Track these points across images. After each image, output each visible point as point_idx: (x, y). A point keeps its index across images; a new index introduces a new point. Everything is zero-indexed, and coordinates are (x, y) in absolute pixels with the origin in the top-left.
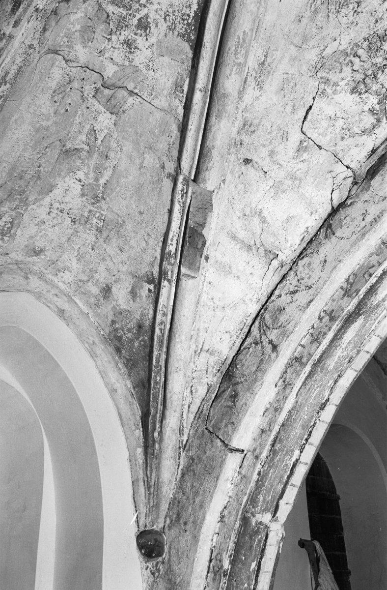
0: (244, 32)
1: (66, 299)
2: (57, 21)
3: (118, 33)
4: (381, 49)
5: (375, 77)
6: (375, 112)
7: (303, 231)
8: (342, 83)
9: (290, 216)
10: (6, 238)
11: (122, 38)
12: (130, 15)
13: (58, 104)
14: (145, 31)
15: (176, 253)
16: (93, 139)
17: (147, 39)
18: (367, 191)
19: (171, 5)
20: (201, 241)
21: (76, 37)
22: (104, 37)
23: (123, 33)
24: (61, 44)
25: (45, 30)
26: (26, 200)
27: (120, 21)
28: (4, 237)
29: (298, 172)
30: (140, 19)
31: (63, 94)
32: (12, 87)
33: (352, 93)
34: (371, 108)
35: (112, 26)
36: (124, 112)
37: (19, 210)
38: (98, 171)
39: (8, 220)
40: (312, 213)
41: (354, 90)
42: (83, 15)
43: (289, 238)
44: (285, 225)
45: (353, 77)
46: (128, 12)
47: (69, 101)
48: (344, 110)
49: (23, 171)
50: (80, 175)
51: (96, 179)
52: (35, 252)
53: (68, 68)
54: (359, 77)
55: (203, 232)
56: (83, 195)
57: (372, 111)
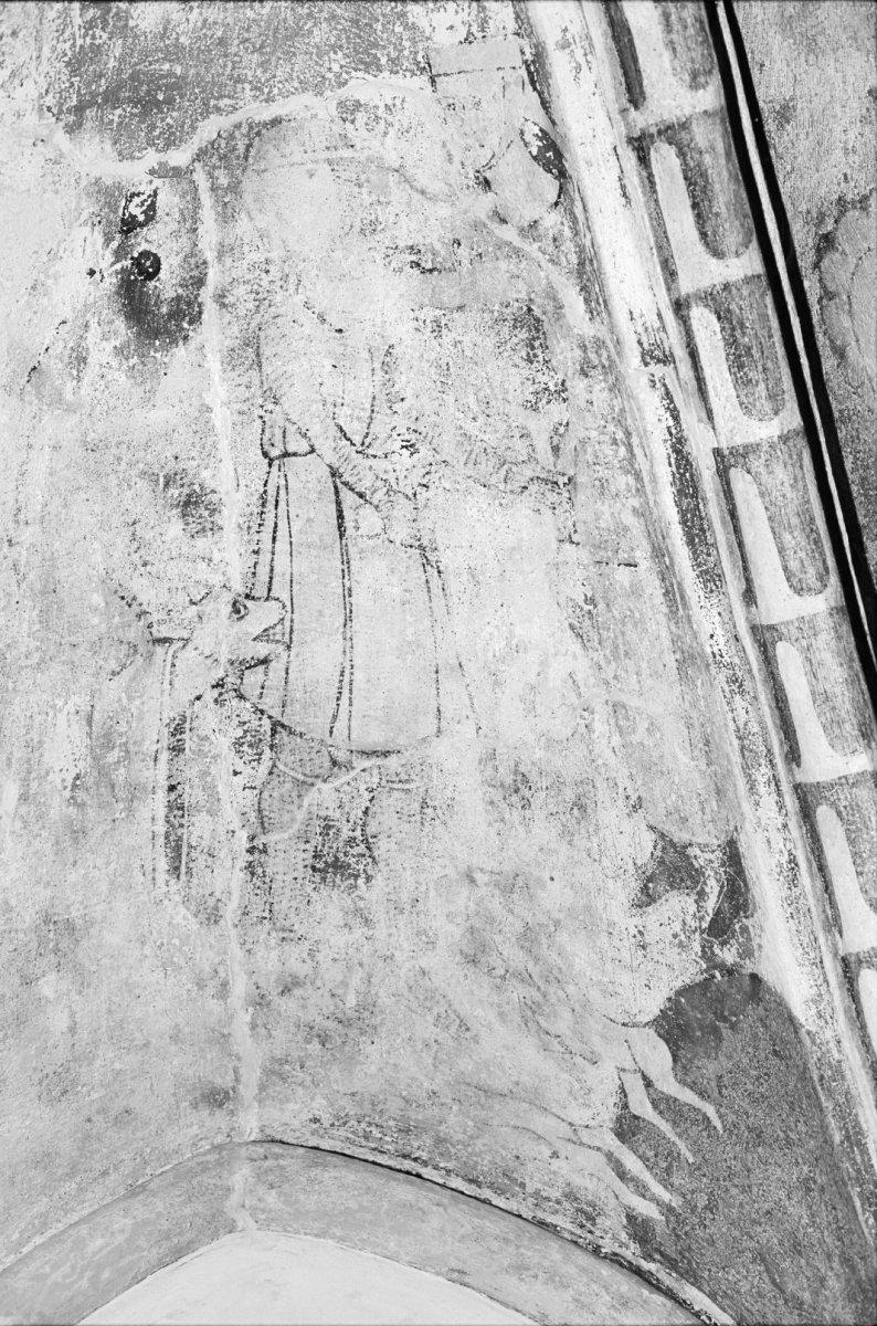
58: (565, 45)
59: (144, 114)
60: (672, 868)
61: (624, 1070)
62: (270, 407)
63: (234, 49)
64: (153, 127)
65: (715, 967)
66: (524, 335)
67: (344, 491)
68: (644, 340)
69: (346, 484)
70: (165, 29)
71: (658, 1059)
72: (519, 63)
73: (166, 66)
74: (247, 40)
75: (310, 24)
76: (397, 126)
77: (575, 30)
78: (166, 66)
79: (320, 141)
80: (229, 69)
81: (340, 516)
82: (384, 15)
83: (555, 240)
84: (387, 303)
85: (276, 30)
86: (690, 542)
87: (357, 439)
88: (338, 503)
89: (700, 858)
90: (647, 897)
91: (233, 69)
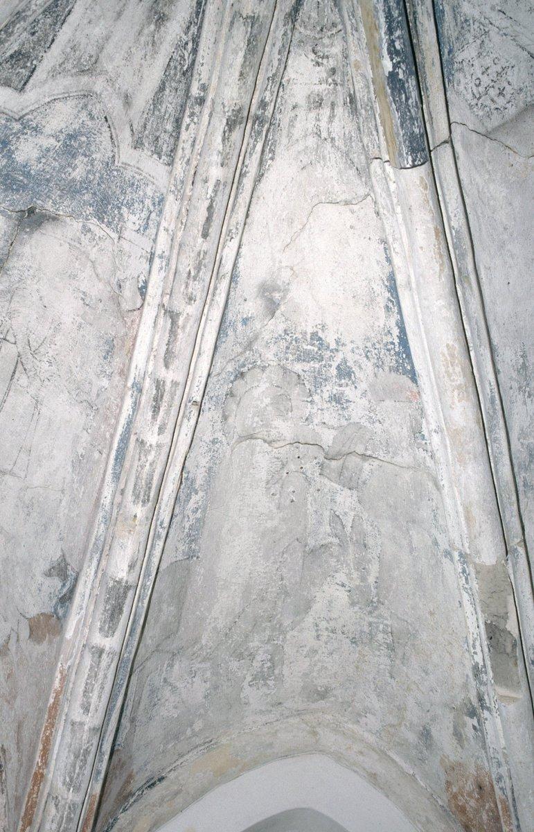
0: (448, 345)
1: (376, 757)
2: (237, 402)
3: (319, 391)
10: (271, 683)
11: (326, 395)
12: (325, 367)
13: (278, 496)
14: (350, 378)
15: (484, 666)
16: (339, 527)
17: (356, 387)
19: (368, 339)
20: (509, 640)
21: (269, 412)
22: (303, 401)
23: (325, 389)
24: (255, 426)
25: (225, 418)
26: (280, 627)
27: (315, 377)
28: (268, 682)
30: (338, 366)
31: (281, 481)
32: (207, 494)
35: (308, 386)
36: (364, 483)
37: (276, 642)
38: (361, 565)
39: (264, 658)
42: (268, 385)
46: (320, 363)
47: (291, 489)
49: (262, 590)
50: (341, 577)
51: (363, 579)
52: (318, 694)
53: (275, 450)
55: (507, 627)
56: (353, 604)
58: (161, 257)
59: (5, 190)
60: (61, 570)
61: (13, 630)
62: (7, 319)
63: (51, 185)
64: (7, 196)
65: (56, 613)
66: (107, 348)
67: (20, 366)
68: (137, 379)
69: (22, 362)
70: (27, 164)
71: (25, 633)
72: (149, 251)
73: (21, 178)
74: (58, 185)
75: (85, 191)
76: (99, 246)
77: (167, 254)
78: (21, 178)
79: (70, 235)
80: (46, 191)
81: (14, 373)
82: (113, 204)
83: (132, 321)
84: (67, 308)
85: (71, 187)
86: (116, 460)
87: (33, 349)
88: (16, 368)
89: (70, 572)
90: (48, 574)
91: (48, 192)
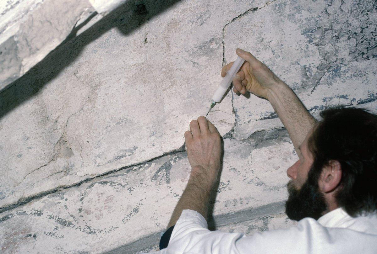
4: (367, 14)
5: (338, 38)
6: (308, 73)
7: (127, 148)
8: (305, 14)
9: (128, 118)
18: (242, 157)
29: (179, 72)
33: (304, 33)
34: (308, 66)
40: (154, 134)
41: (309, 31)
43: (104, 145)
44: (113, 124)
45: (320, 17)
48: (282, 45)
54: (325, 22)
57: (305, 69)
